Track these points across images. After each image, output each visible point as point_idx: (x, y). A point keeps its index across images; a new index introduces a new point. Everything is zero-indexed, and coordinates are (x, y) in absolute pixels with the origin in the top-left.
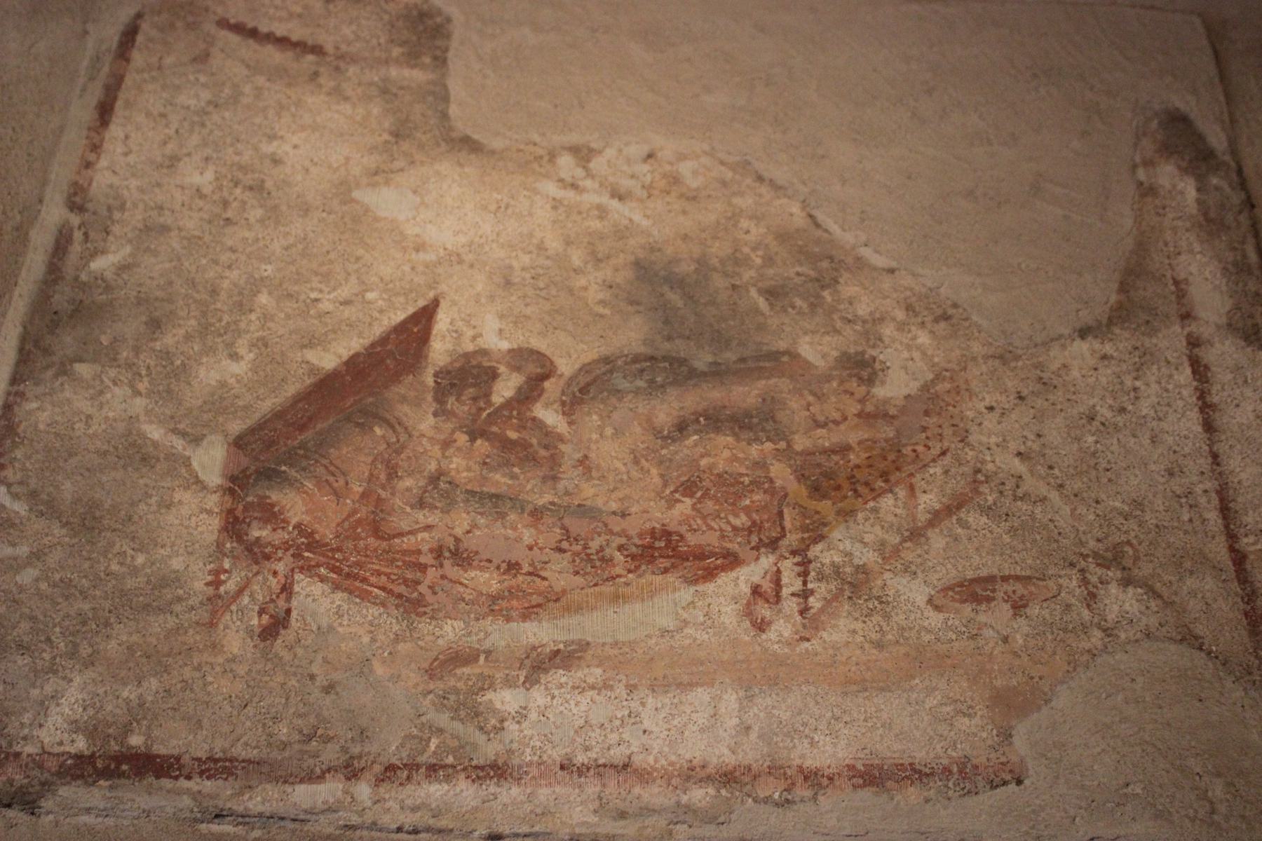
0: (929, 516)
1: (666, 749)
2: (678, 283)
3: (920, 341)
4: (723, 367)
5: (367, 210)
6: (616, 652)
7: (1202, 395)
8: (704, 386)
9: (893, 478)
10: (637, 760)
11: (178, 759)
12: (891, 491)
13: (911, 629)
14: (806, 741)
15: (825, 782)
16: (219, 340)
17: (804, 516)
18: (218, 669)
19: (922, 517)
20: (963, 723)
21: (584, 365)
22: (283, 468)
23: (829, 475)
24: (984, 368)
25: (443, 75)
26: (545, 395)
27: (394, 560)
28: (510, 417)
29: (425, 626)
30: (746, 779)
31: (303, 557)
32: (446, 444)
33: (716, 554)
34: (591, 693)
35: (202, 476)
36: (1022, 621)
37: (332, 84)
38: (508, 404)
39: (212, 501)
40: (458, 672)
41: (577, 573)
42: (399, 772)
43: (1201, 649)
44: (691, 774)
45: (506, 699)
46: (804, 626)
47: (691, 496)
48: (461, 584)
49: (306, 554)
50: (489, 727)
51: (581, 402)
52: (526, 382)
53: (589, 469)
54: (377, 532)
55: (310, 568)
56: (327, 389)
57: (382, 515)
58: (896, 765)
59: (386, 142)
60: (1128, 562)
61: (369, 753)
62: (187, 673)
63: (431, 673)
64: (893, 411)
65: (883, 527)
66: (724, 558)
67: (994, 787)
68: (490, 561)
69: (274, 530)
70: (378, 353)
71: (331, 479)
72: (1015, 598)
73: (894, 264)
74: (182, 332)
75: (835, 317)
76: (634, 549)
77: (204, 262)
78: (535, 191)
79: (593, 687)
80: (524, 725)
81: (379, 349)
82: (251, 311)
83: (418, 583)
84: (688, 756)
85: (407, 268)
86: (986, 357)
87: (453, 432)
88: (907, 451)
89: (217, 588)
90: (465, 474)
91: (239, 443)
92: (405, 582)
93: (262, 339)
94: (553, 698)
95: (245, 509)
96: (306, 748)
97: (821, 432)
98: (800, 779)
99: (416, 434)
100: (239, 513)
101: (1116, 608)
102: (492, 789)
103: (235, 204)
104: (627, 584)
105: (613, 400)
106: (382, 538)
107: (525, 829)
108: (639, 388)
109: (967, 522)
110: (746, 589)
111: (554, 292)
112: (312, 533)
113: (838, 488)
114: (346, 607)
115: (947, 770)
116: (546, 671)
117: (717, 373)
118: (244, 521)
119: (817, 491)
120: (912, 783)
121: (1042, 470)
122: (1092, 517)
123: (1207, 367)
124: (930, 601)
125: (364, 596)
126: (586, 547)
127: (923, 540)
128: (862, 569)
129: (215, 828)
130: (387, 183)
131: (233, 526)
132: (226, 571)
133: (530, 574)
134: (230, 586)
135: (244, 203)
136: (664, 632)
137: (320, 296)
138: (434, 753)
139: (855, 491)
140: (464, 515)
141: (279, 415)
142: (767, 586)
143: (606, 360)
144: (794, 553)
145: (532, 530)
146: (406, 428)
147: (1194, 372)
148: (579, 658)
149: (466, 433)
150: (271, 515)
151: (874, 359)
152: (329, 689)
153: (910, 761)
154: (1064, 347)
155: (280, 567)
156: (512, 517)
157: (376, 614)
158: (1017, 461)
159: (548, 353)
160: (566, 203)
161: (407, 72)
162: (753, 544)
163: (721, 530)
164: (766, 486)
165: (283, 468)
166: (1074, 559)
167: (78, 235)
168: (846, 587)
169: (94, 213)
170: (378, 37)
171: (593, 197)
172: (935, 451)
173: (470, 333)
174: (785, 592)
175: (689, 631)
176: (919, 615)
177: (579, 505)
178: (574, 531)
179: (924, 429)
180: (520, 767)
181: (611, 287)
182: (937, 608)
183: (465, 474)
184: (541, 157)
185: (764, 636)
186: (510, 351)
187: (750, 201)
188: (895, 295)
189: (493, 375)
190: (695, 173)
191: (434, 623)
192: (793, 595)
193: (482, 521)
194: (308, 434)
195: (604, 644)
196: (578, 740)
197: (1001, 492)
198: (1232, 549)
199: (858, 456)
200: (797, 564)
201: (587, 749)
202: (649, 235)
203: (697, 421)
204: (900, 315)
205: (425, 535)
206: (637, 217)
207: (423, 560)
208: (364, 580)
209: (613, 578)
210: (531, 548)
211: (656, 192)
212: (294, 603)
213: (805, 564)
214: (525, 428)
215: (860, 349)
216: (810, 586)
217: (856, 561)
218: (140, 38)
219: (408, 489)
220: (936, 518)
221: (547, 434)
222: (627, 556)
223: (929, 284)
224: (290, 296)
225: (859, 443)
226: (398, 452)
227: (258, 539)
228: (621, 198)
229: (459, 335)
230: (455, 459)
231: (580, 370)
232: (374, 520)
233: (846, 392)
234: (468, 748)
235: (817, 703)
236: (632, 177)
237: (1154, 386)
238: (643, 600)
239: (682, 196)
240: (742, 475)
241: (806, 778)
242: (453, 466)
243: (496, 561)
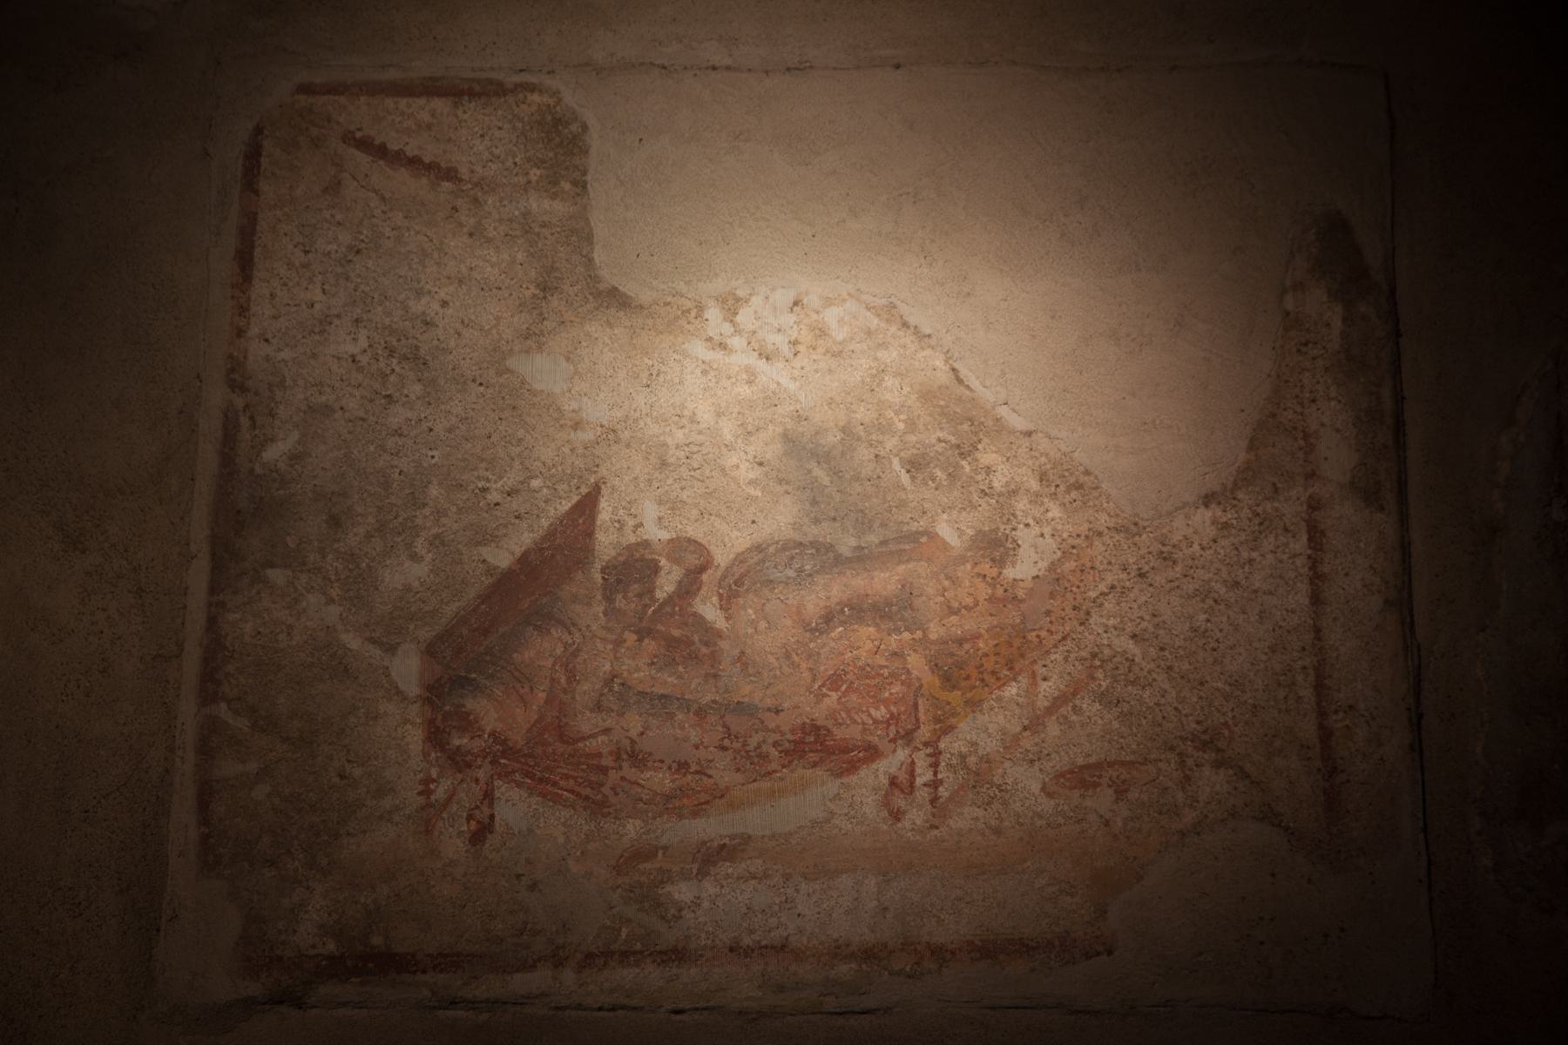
0: (1046, 704)
2: (824, 457)
3: (1050, 515)
7: (1314, 563)
8: (848, 573)
9: (1017, 667)
12: (1015, 679)
15: (948, 956)
19: (1042, 703)
23: (960, 665)
25: (585, 208)
28: (672, 615)
32: (619, 643)
35: (402, 687)
37: (472, 221)
38: (670, 600)
40: (641, 867)
41: (738, 770)
43: (1279, 826)
44: (838, 951)
47: (836, 690)
51: (737, 595)
52: (686, 575)
53: (745, 666)
55: (507, 774)
60: (1222, 744)
64: (1021, 594)
73: (1032, 427)
74: (361, 530)
75: (972, 489)
78: (685, 355)
82: (425, 505)
83: (602, 785)
84: (835, 936)
85: (566, 450)
88: (1032, 636)
91: (430, 651)
92: (591, 785)
93: (437, 536)
97: (954, 619)
100: (439, 722)
101: (1208, 790)
102: (674, 971)
105: (766, 592)
106: (567, 743)
107: (702, 1004)
110: (886, 782)
111: (707, 473)
113: (968, 678)
116: (715, 863)
117: (861, 559)
121: (1153, 652)
123: (1323, 533)
124: (1043, 789)
126: (745, 745)
129: (450, 1013)
130: (540, 348)
131: (435, 737)
133: (697, 772)
134: (440, 793)
136: (814, 823)
139: (983, 680)
142: (903, 777)
143: (758, 548)
144: (926, 744)
147: (1310, 539)
150: (467, 723)
152: (533, 887)
155: (481, 774)
156: (680, 716)
159: (704, 542)
161: (546, 204)
167: (244, 421)
169: (256, 394)
170: (514, 156)
171: (742, 358)
173: (631, 522)
174: (919, 781)
179: (1048, 613)
181: (761, 464)
182: (1050, 795)
184: (689, 311)
189: (655, 569)
190: (841, 321)
193: (654, 722)
198: (1321, 727)
201: (751, 932)
202: (797, 401)
203: (842, 611)
204: (1034, 485)
206: (784, 381)
207: (604, 762)
208: (555, 784)
211: (801, 348)
213: (937, 754)
214: (686, 624)
218: (264, 161)
223: (1063, 448)
226: (575, 654)
227: (459, 747)
237: (1269, 556)
240: (882, 667)
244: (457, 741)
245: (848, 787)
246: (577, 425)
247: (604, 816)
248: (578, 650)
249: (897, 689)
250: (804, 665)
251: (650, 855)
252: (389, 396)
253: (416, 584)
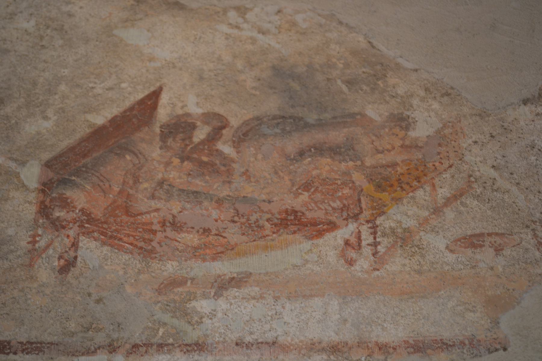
0: (444, 201)
1: (298, 333)
3: (433, 107)
4: (324, 122)
5: (121, 40)
6: (267, 278)
9: (422, 180)
10: (280, 339)
11: (9, 343)
12: (422, 187)
13: (437, 263)
14: (379, 327)
15: (391, 350)
16: (37, 109)
17: (373, 201)
18: (34, 291)
20: (470, 316)
21: (245, 121)
22: (73, 178)
23: (386, 179)
24: (471, 121)
26: (224, 137)
27: (137, 228)
28: (203, 150)
29: (155, 265)
30: (345, 349)
31: (85, 227)
32: (168, 164)
33: (324, 223)
34: (253, 301)
35: (26, 183)
36: (501, 258)
38: (202, 142)
39: (32, 197)
40: (176, 290)
41: (244, 234)
42: (141, 349)
45: (203, 306)
46: (375, 262)
47: (308, 191)
48: (176, 241)
49: (86, 225)
50: (194, 321)
51: (244, 141)
53: (249, 177)
54: (127, 212)
56: (99, 135)
57: (130, 203)
58: (433, 341)
59: (132, 5)
61: (123, 337)
62: (16, 293)
63: (159, 291)
64: (420, 144)
65: (418, 207)
66: (328, 225)
67: (490, 352)
68: (193, 228)
69: (68, 212)
70: (128, 116)
71: (101, 184)
72: (496, 245)
73: (417, 67)
74: (15, 105)
76: (276, 221)
77: (29, 68)
79: (254, 298)
80: (214, 320)
81: (128, 113)
82: (55, 94)
83: (152, 241)
85: (144, 70)
86: (472, 115)
87: (171, 158)
88: (430, 165)
89: (34, 245)
90: (178, 180)
92: (144, 240)
93: (61, 108)
94: (231, 304)
95: (51, 201)
96: (87, 335)
97: (380, 156)
98: (377, 350)
99: (150, 159)
100: (47, 203)
103: (46, 38)
104: (273, 240)
106: (131, 216)
108: (276, 133)
109: (466, 204)
110: (341, 242)
112: (90, 214)
113: (392, 186)
114: (109, 255)
115: (462, 343)
116: (226, 289)
117: (321, 125)
118: (50, 208)
119: (379, 187)
120: (443, 350)
122: (537, 200)
124: (447, 248)
125: (120, 248)
126: (248, 220)
127: (441, 213)
128: (407, 230)
130: (133, 26)
131: (44, 210)
132: (39, 235)
133: (216, 235)
134: (42, 243)
135: (52, 37)
136: (295, 266)
137: (95, 85)
138: (162, 337)
139: (402, 187)
140: (178, 203)
141: (71, 149)
142: (353, 240)
143: (258, 118)
144: (368, 222)
145: (217, 211)
146: (144, 156)
148: (246, 282)
149: (178, 158)
150: (65, 204)
151: (409, 117)
152: (99, 301)
153: (441, 338)
154: (514, 109)
155: (71, 233)
156: (206, 203)
157: (127, 258)
158: (492, 170)
159: (224, 115)
160: (233, 36)
162: (344, 217)
163: (326, 209)
164: (351, 185)
165: (73, 178)
166: (529, 223)
168: (399, 240)
172: (446, 165)
173: (180, 105)
174: (364, 243)
175: (309, 266)
176: (441, 255)
177: (244, 197)
178: (241, 211)
179: (439, 153)
180: (212, 344)
181: (259, 80)
182: (452, 251)
183: (178, 180)
184: (219, 12)
185: (353, 268)
186: (203, 114)
187: (336, 35)
188: (418, 83)
189: (194, 127)
190: (304, 20)
191: (161, 263)
192: (368, 245)
193: (188, 206)
194: (88, 160)
195: (260, 274)
196: (246, 328)
197: (484, 187)
199: (402, 168)
200: (370, 228)
201: (251, 333)
203: (310, 150)
204: (422, 93)
205: (156, 214)
206: (273, 43)
207: (154, 228)
208: (120, 239)
209: (264, 237)
210: (216, 221)
212: (79, 253)
214: (212, 155)
215: (400, 111)
216: (378, 240)
217: (404, 226)
219: (146, 189)
220: (448, 202)
221: (225, 158)
222: (272, 224)
224: (78, 86)
225: (402, 161)
226: (139, 169)
227: (58, 217)
228: (263, 33)
229: (174, 105)
230: (172, 172)
231: (243, 124)
232: (126, 207)
233: (393, 134)
234: (181, 334)
235: (385, 305)
236: (270, 22)
238: (282, 249)
239: (297, 32)
240: (336, 179)
241: (380, 349)
242: (171, 176)
243: (197, 228)
244: (58, 213)
245: (317, 246)
246: (151, 59)
247: (151, 258)
249: (346, 191)
250: (286, 178)
251: (182, 282)
252: (43, 46)
253: (45, 131)
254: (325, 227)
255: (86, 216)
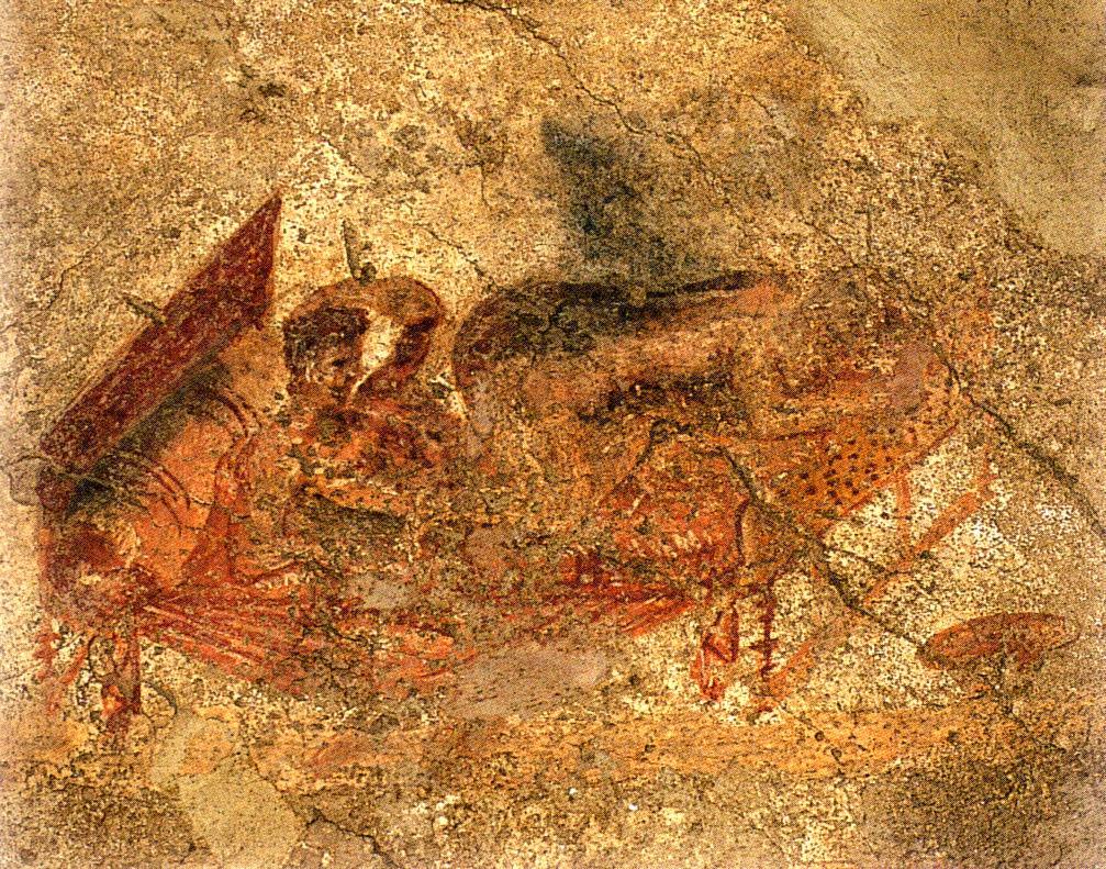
66: (670, 596)
113: (812, 490)
144: (753, 589)
146: (255, 415)
174: (743, 643)
176: (905, 673)
189: (364, 327)
216: (773, 635)
248: (253, 444)
254: (660, 604)
255: (146, 585)
